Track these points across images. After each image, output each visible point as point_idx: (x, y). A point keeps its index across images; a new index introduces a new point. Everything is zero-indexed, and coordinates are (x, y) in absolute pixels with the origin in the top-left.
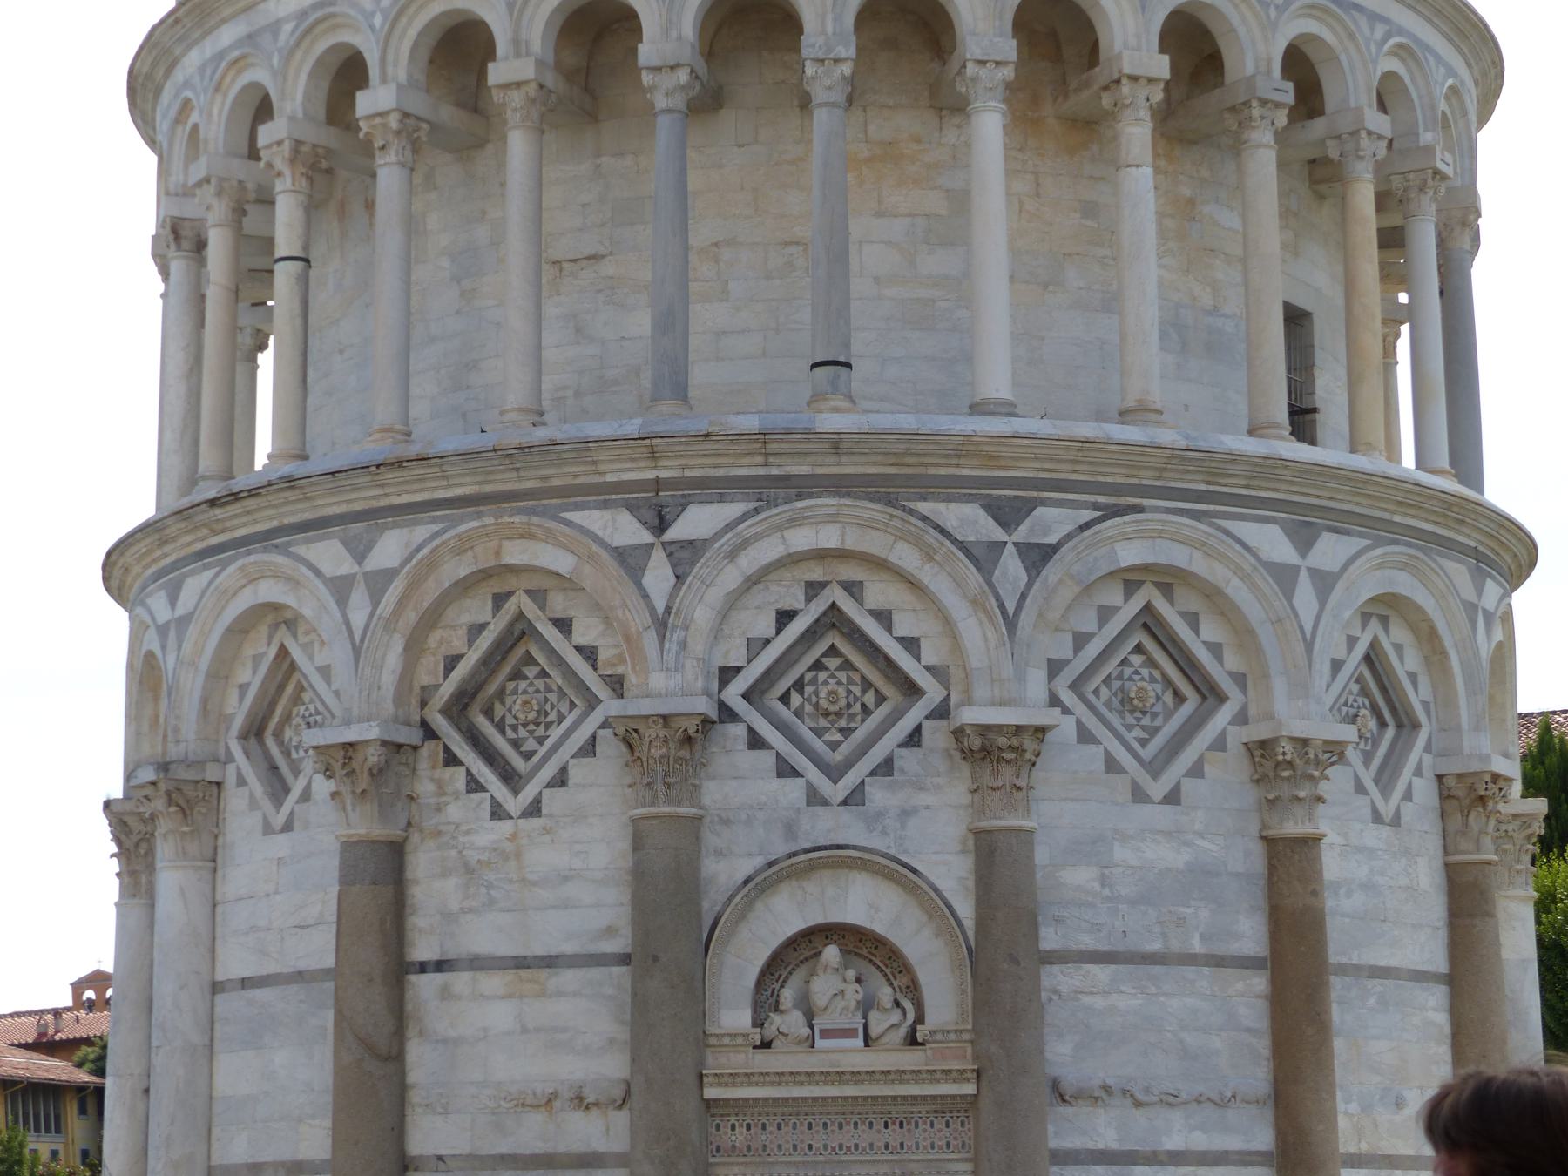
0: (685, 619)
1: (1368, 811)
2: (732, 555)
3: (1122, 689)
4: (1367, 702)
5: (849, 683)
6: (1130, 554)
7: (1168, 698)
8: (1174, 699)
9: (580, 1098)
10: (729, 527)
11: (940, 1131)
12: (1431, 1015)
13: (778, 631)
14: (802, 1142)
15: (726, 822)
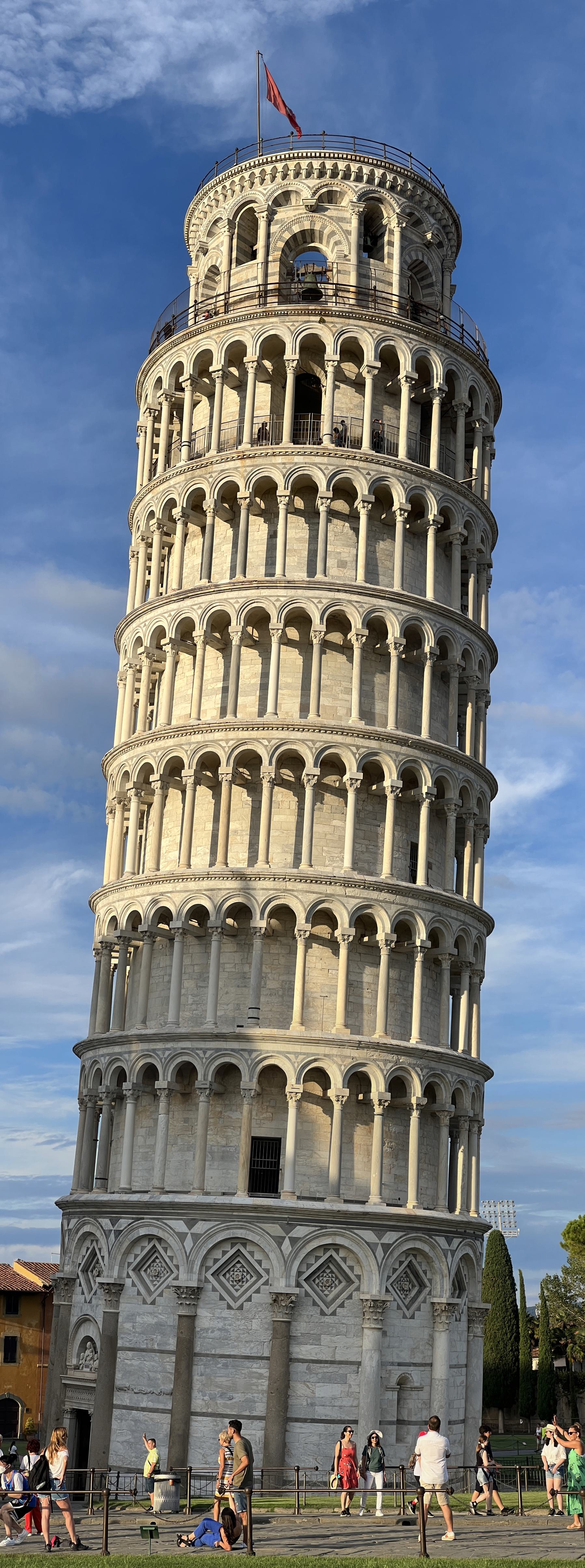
6: (142, 1232)
7: (165, 1272)
12: (254, 1370)
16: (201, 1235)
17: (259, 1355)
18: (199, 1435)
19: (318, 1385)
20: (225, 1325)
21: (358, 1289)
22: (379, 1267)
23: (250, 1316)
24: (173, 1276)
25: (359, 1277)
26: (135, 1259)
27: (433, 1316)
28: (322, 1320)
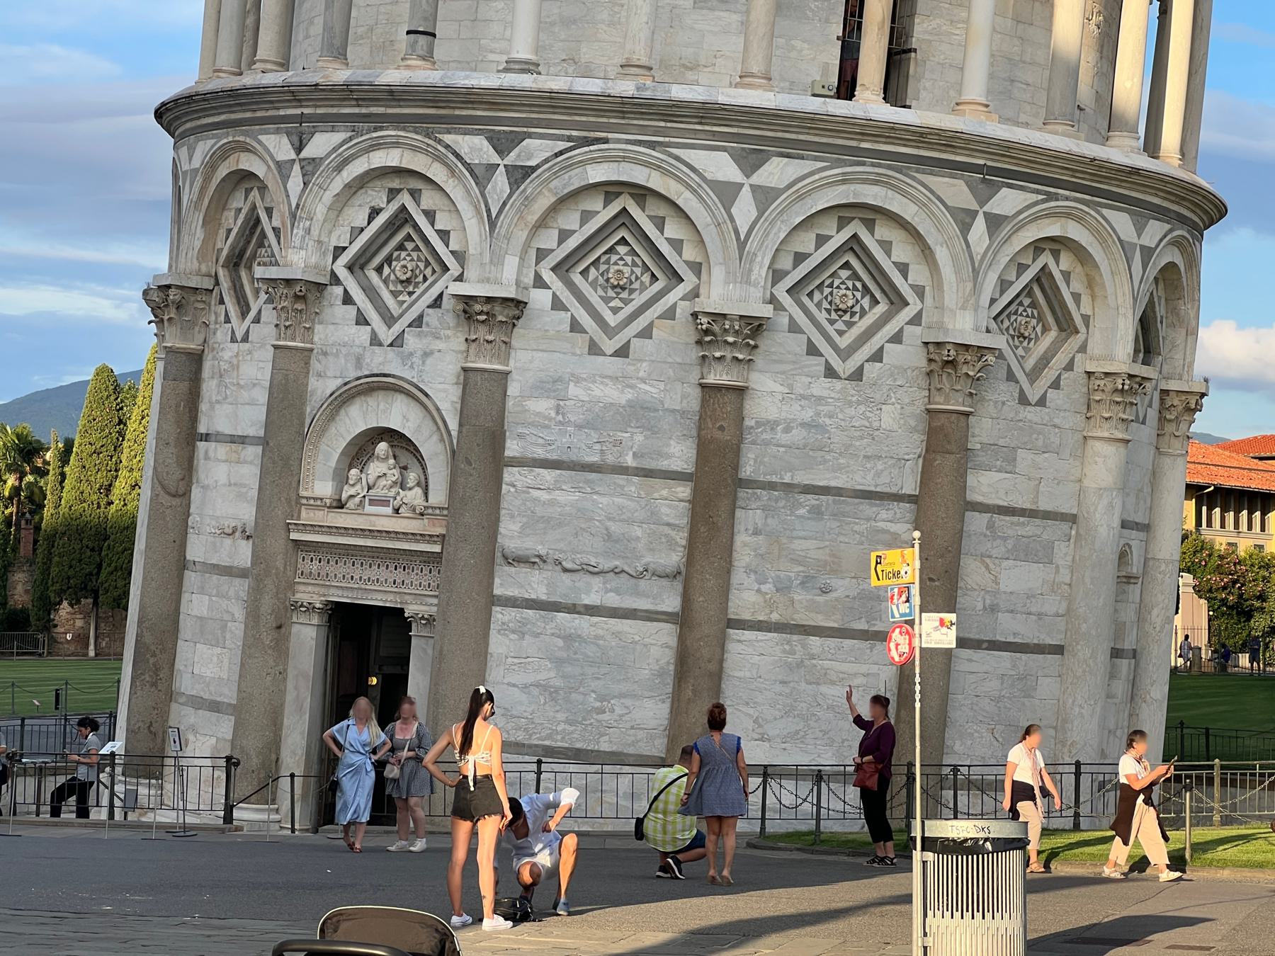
0: (309, 212)
1: (822, 369)
2: (339, 169)
3: (607, 271)
4: (859, 285)
5: (418, 261)
6: (597, 174)
7: (646, 278)
8: (651, 278)
9: (244, 531)
10: (335, 150)
11: (426, 575)
12: (881, 525)
13: (369, 224)
14: (348, 574)
15: (325, 354)
16: (777, 192)
17: (894, 490)
18: (748, 674)
19: (1005, 563)
20: (818, 414)
21: (1083, 349)
22: (1135, 299)
23: (878, 396)
24: (680, 290)
25: (1086, 319)
26: (560, 242)
27: (1162, 420)
28: (1021, 416)
